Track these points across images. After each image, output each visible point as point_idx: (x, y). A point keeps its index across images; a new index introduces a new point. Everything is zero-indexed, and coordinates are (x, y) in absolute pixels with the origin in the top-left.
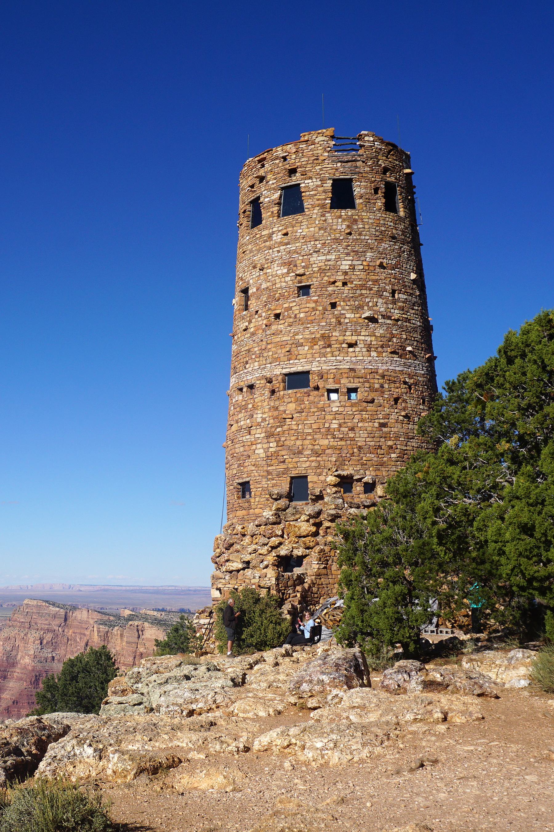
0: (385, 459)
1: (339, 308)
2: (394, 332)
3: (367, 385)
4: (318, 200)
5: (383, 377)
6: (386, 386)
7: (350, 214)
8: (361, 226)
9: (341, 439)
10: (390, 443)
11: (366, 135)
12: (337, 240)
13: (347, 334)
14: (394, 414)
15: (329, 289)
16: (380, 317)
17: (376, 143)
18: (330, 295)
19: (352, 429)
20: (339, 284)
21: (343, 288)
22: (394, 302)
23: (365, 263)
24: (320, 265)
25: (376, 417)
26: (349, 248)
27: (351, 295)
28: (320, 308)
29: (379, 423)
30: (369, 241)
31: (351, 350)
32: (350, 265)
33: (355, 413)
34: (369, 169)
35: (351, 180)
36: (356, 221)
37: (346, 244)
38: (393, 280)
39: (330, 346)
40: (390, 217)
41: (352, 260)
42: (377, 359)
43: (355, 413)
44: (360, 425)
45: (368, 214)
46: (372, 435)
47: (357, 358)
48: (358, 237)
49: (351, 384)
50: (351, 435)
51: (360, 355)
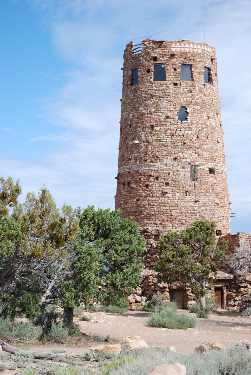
0: (138, 218)
1: (127, 140)
2: (149, 149)
3: (134, 180)
4: (126, 82)
5: (141, 175)
6: (142, 179)
7: (135, 87)
8: (138, 93)
9: (123, 209)
10: (140, 209)
11: (145, 41)
12: (130, 104)
13: (129, 153)
14: (144, 193)
15: (126, 130)
16: (142, 142)
17: (150, 44)
18: (125, 133)
19: (126, 203)
20: (128, 127)
21: (129, 129)
22: (151, 133)
23: (138, 114)
24: (125, 117)
25: (136, 196)
26: (133, 106)
27: (131, 132)
28: (123, 141)
29: (137, 199)
30: (141, 101)
31: (130, 161)
32: (133, 116)
33: (128, 195)
34: (144, 60)
35: (137, 69)
36: (136, 91)
37: (132, 104)
38: (151, 120)
39: (124, 160)
40: (155, 84)
41: (134, 113)
42: (139, 165)
43: (128, 195)
44: (129, 201)
45: (142, 86)
46: (133, 206)
47: (132, 166)
48: (137, 100)
49: (128, 180)
50: (126, 207)
51: (132, 164)
